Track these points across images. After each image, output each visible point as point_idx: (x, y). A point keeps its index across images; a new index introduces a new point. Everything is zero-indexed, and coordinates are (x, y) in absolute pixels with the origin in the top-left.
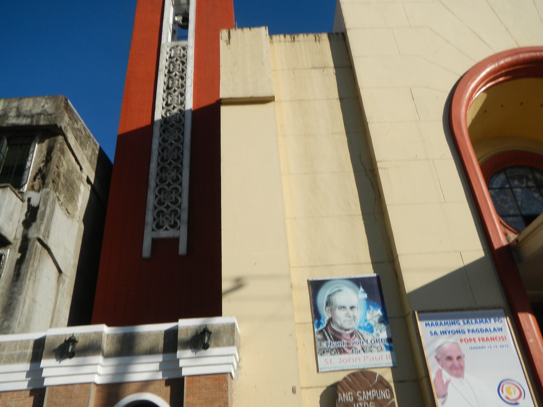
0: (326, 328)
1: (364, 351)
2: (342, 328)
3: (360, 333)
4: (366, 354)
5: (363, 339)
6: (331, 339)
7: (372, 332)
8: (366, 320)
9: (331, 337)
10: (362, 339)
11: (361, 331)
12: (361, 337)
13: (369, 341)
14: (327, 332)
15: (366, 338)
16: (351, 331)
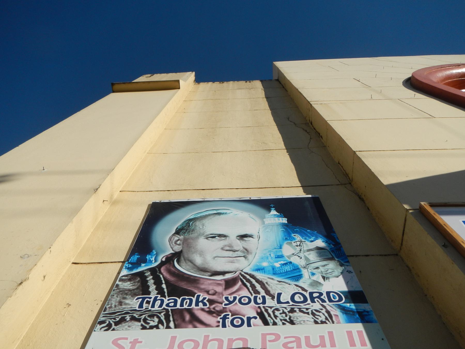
0: (153, 271)
1: (266, 323)
2: (203, 270)
3: (258, 281)
4: (270, 329)
5: (267, 292)
6: (160, 292)
7: (299, 277)
8: (281, 257)
9: (164, 286)
10: (263, 293)
11: (259, 276)
12: (258, 287)
13: (285, 297)
14: (158, 283)
15: (275, 292)
16: (228, 276)
